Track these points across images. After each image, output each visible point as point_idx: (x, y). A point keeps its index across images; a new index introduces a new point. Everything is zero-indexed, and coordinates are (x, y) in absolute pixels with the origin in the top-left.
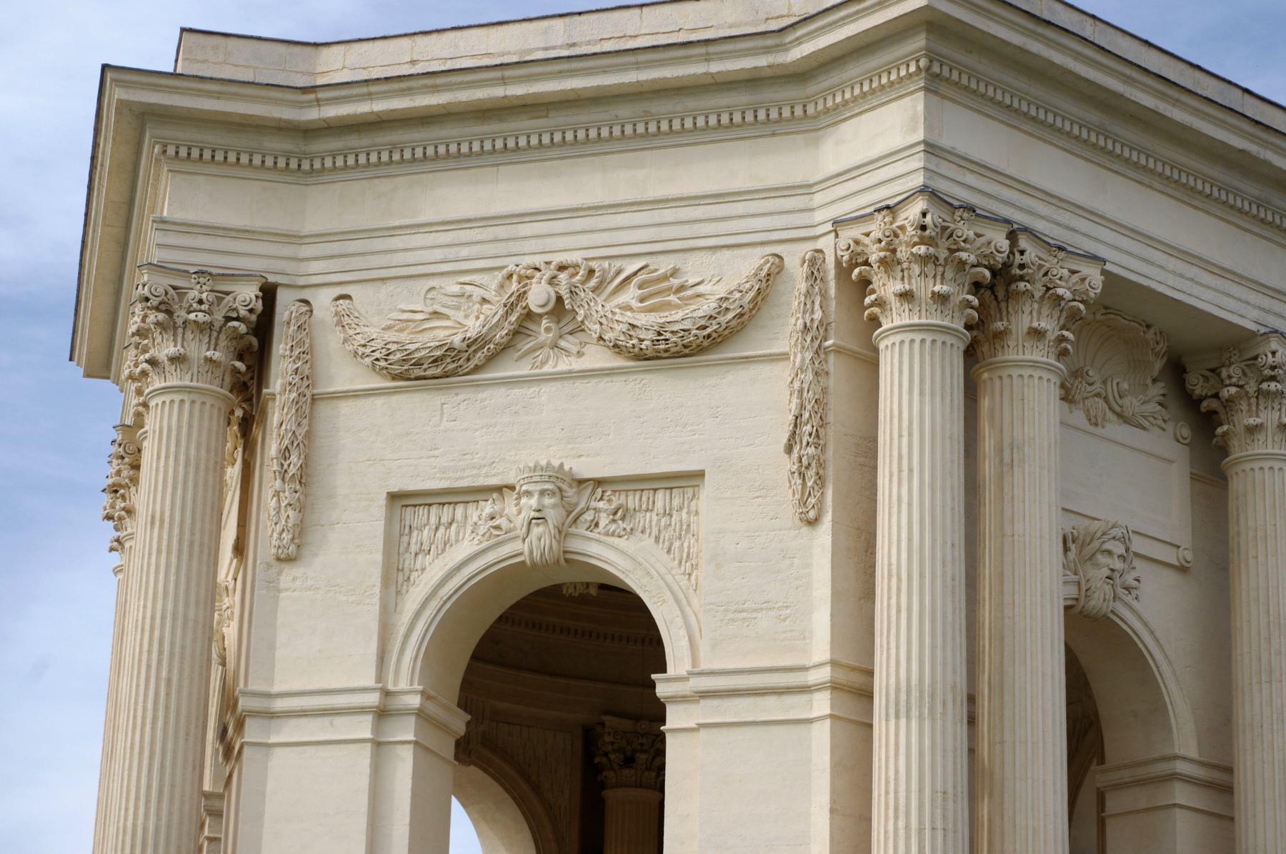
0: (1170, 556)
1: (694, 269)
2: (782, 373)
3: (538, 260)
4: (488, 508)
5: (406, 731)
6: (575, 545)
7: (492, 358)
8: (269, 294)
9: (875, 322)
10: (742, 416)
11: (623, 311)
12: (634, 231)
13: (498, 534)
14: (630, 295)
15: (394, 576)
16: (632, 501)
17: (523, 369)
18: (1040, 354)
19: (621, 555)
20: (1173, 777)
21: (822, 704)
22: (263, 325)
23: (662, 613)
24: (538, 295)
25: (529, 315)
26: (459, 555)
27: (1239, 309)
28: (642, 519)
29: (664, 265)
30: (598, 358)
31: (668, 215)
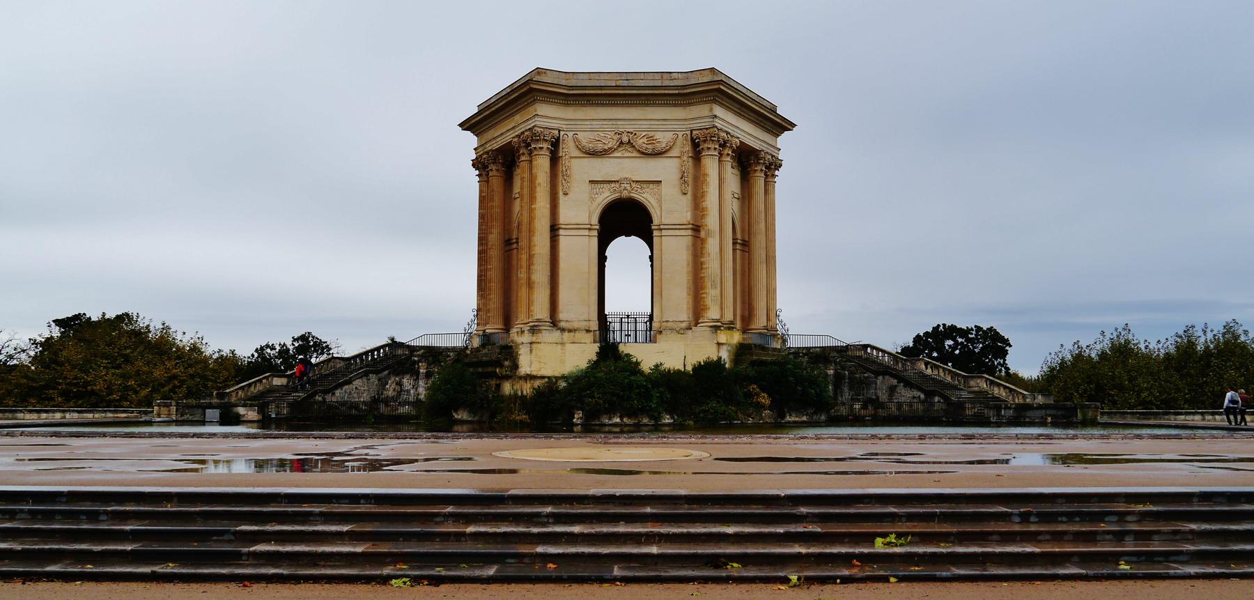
1: (658, 136)
5: (596, 233)
9: (700, 152)
10: (667, 170)
14: (645, 140)
15: (592, 199)
17: (619, 154)
18: (729, 159)
21: (689, 232)
22: (558, 140)
23: (652, 211)
24: (625, 139)
25: (621, 143)
26: (606, 196)
27: (756, 145)
29: (651, 134)
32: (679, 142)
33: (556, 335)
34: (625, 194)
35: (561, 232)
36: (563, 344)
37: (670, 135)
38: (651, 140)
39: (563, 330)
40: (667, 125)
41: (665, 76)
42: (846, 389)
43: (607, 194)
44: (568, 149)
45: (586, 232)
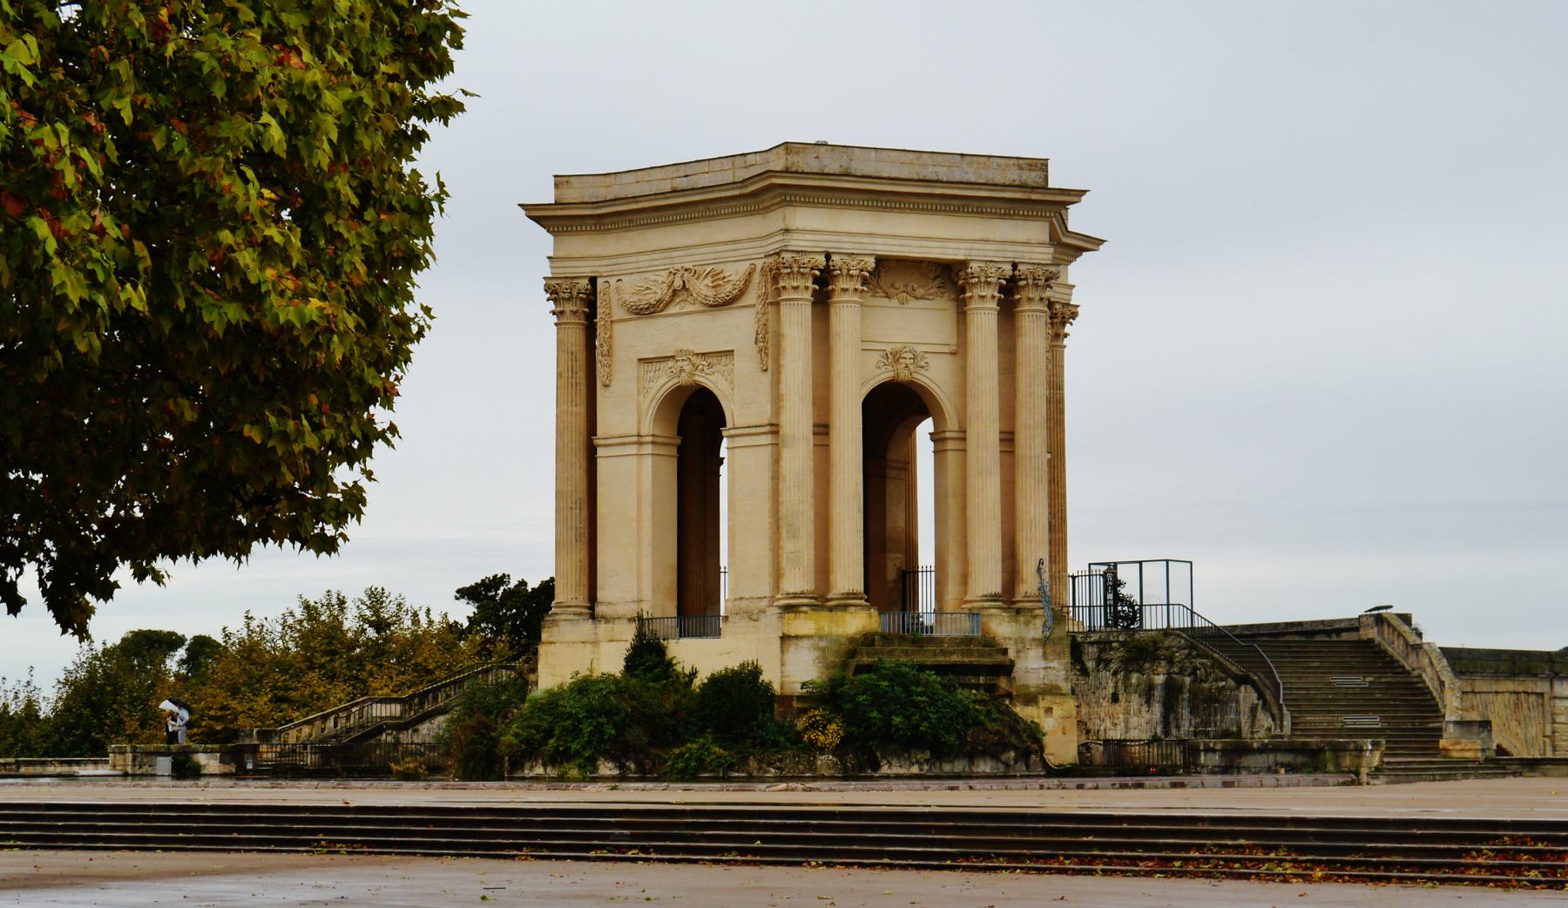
0: (946, 349)
2: (752, 311)
3: (678, 266)
4: (670, 363)
6: (697, 378)
7: (667, 305)
8: (593, 281)
11: (702, 287)
12: (706, 254)
13: (673, 375)
14: (708, 281)
16: (714, 360)
19: (714, 381)
20: (946, 439)
24: (678, 283)
26: (662, 382)
28: (718, 367)
29: (718, 268)
30: (698, 307)
31: (719, 248)
32: (757, 278)
33: (587, 626)
34: (684, 379)
35: (600, 452)
36: (595, 643)
37: (744, 267)
38: (717, 278)
39: (607, 619)
40: (734, 245)
41: (739, 161)
42: (1185, 713)
43: (664, 380)
44: (610, 306)
45: (633, 449)
